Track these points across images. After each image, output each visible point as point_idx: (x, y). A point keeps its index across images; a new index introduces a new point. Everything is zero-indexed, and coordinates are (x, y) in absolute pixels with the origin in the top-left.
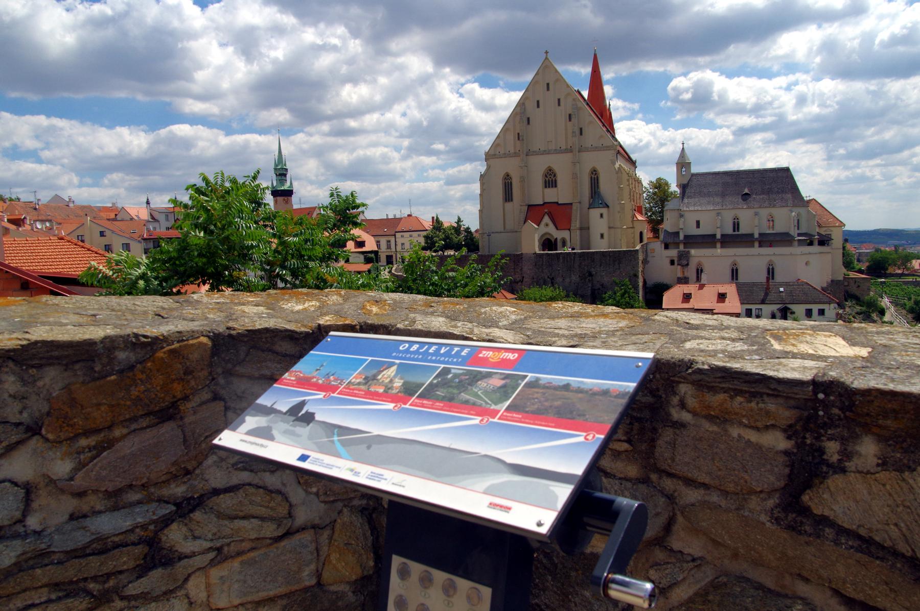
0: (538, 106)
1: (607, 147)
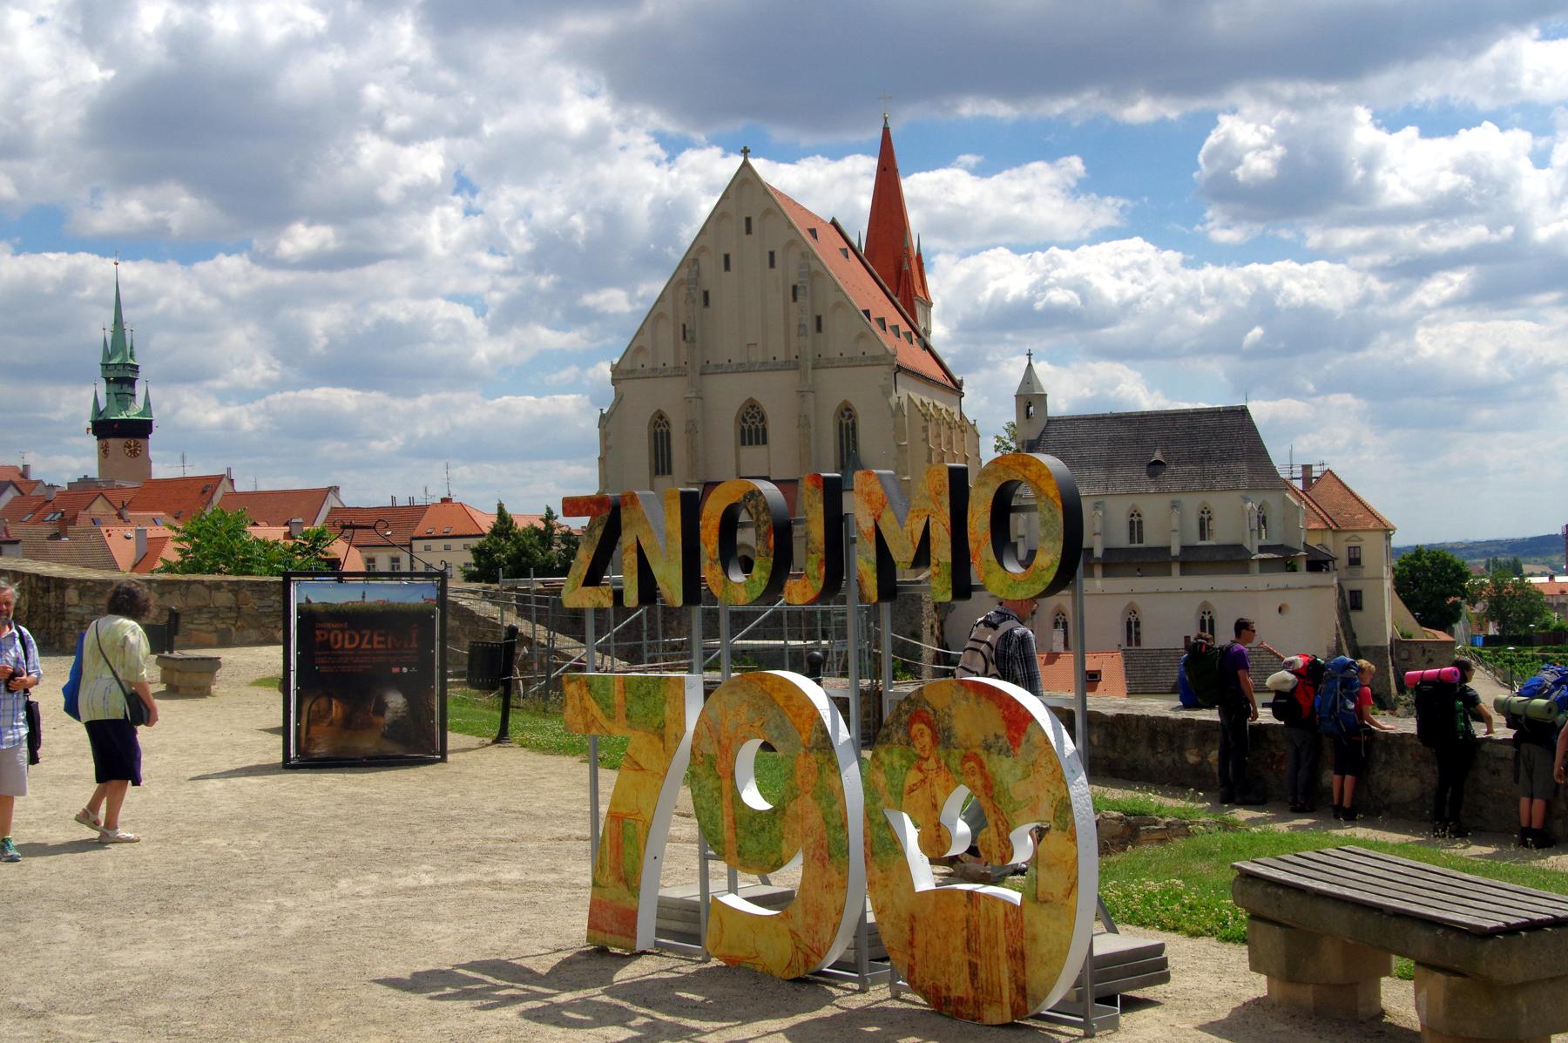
0: (727, 267)
1: (874, 358)
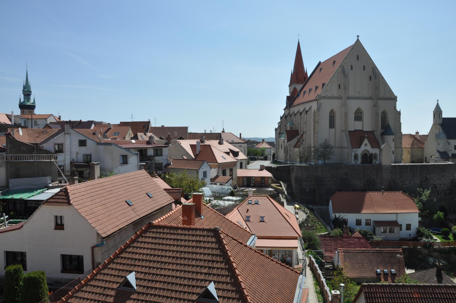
0: (352, 69)
